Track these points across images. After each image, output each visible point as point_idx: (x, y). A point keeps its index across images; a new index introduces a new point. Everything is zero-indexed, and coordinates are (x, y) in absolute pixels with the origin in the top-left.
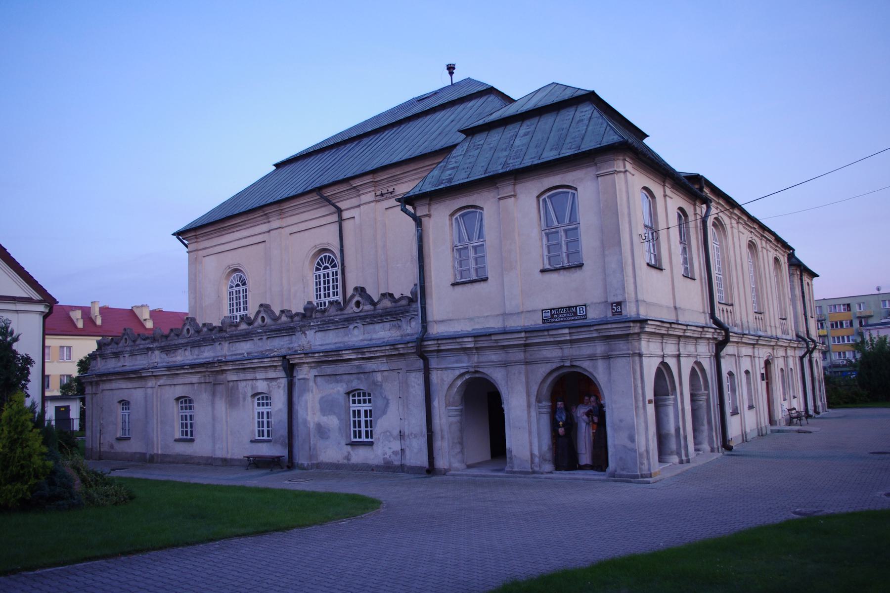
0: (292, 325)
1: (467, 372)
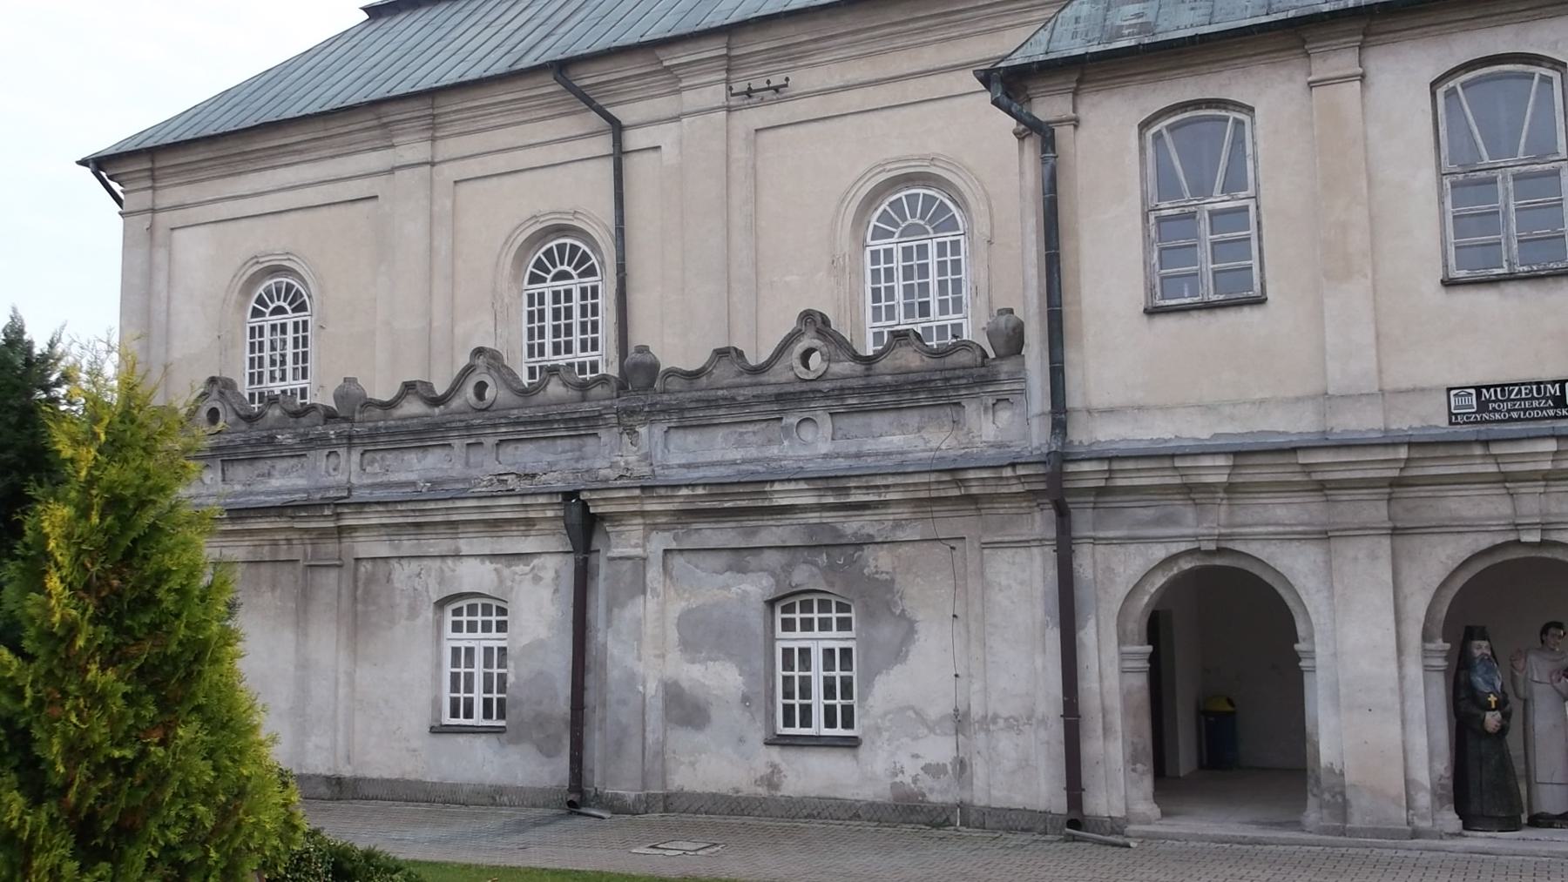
0: (586, 406)
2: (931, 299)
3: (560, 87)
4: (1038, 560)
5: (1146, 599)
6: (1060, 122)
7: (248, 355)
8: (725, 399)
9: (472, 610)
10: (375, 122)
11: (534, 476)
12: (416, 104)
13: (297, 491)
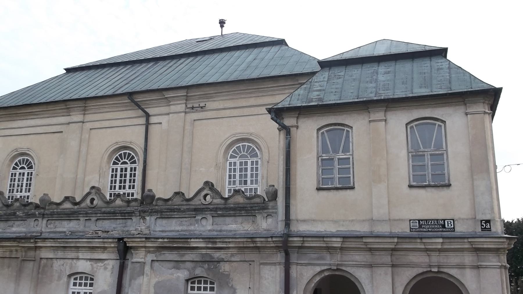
1: (330, 269)
2: (248, 179)
3: (129, 101)
4: (278, 270)
5: (313, 285)
6: (292, 126)
7: (9, 183)
8: (177, 209)
9: (81, 278)
10: (65, 107)
11: (108, 232)
12: (79, 102)
13: (22, 233)
